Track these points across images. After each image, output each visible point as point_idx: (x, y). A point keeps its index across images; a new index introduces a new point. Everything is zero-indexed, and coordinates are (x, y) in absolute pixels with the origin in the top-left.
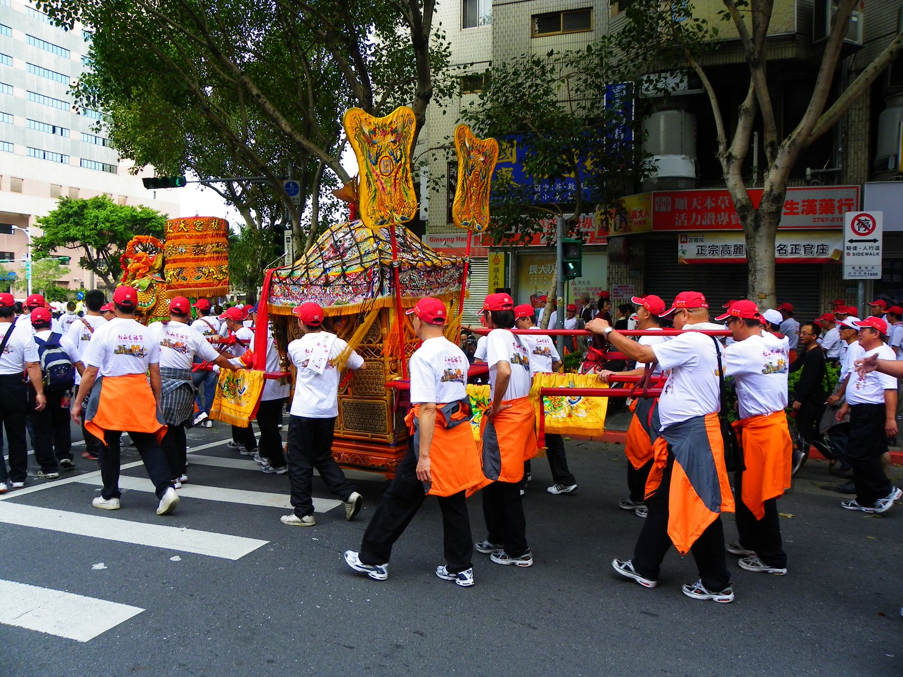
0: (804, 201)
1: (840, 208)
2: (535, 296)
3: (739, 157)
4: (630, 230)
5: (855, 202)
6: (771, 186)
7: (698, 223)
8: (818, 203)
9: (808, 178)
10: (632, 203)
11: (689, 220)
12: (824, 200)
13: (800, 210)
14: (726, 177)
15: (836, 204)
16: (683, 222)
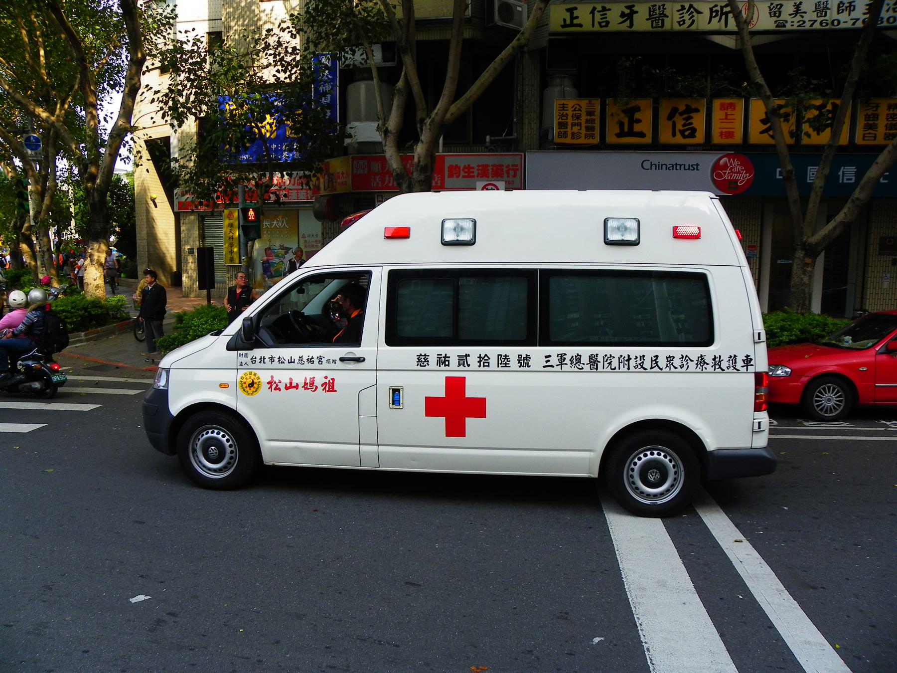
0: (479, 166)
1: (508, 172)
2: (269, 249)
3: (393, 131)
4: (335, 190)
5: (519, 167)
6: (419, 158)
7: (391, 185)
8: (490, 168)
9: (488, 144)
10: (337, 165)
11: (383, 181)
12: (495, 166)
13: (476, 174)
14: (385, 148)
15: (505, 169)
16: (378, 184)
